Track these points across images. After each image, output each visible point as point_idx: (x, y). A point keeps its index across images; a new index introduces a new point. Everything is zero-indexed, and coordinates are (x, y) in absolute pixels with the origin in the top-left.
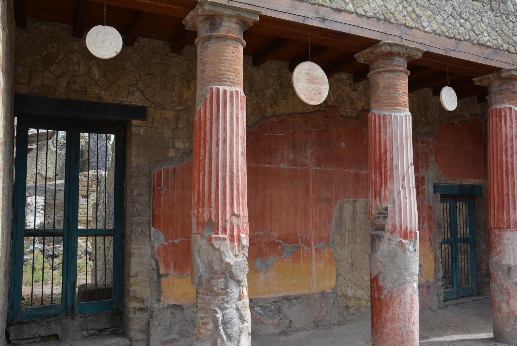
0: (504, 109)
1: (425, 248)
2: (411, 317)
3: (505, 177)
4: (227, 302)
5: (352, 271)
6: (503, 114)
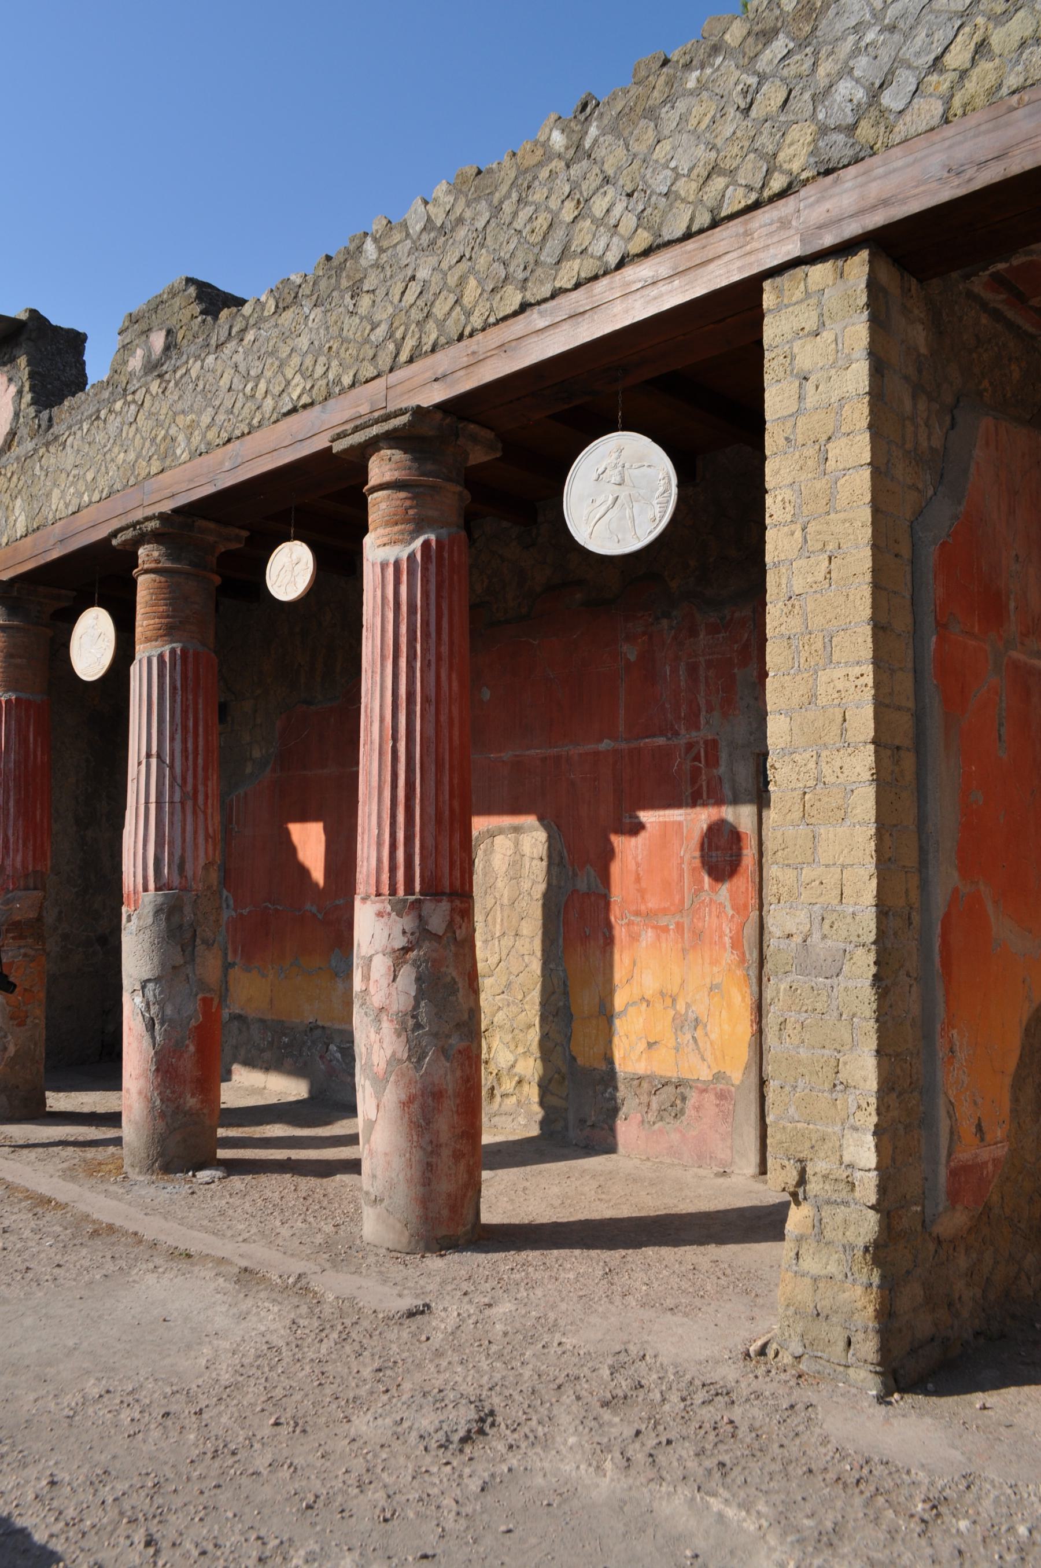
1: (715, 969)
5: (508, 1005)
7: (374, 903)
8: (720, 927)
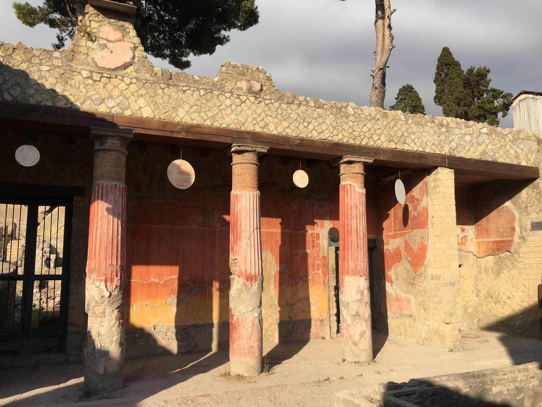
0: (346, 185)
1: (319, 290)
2: (252, 336)
3: (346, 235)
4: (104, 321)
6: (346, 189)
7: (364, 277)
8: (320, 279)
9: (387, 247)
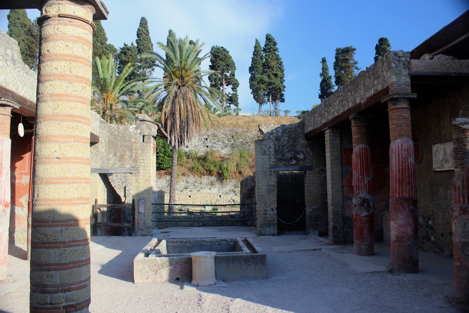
9: (19, 181)
